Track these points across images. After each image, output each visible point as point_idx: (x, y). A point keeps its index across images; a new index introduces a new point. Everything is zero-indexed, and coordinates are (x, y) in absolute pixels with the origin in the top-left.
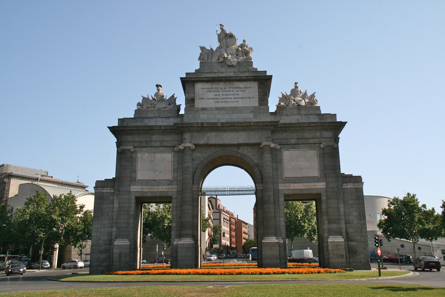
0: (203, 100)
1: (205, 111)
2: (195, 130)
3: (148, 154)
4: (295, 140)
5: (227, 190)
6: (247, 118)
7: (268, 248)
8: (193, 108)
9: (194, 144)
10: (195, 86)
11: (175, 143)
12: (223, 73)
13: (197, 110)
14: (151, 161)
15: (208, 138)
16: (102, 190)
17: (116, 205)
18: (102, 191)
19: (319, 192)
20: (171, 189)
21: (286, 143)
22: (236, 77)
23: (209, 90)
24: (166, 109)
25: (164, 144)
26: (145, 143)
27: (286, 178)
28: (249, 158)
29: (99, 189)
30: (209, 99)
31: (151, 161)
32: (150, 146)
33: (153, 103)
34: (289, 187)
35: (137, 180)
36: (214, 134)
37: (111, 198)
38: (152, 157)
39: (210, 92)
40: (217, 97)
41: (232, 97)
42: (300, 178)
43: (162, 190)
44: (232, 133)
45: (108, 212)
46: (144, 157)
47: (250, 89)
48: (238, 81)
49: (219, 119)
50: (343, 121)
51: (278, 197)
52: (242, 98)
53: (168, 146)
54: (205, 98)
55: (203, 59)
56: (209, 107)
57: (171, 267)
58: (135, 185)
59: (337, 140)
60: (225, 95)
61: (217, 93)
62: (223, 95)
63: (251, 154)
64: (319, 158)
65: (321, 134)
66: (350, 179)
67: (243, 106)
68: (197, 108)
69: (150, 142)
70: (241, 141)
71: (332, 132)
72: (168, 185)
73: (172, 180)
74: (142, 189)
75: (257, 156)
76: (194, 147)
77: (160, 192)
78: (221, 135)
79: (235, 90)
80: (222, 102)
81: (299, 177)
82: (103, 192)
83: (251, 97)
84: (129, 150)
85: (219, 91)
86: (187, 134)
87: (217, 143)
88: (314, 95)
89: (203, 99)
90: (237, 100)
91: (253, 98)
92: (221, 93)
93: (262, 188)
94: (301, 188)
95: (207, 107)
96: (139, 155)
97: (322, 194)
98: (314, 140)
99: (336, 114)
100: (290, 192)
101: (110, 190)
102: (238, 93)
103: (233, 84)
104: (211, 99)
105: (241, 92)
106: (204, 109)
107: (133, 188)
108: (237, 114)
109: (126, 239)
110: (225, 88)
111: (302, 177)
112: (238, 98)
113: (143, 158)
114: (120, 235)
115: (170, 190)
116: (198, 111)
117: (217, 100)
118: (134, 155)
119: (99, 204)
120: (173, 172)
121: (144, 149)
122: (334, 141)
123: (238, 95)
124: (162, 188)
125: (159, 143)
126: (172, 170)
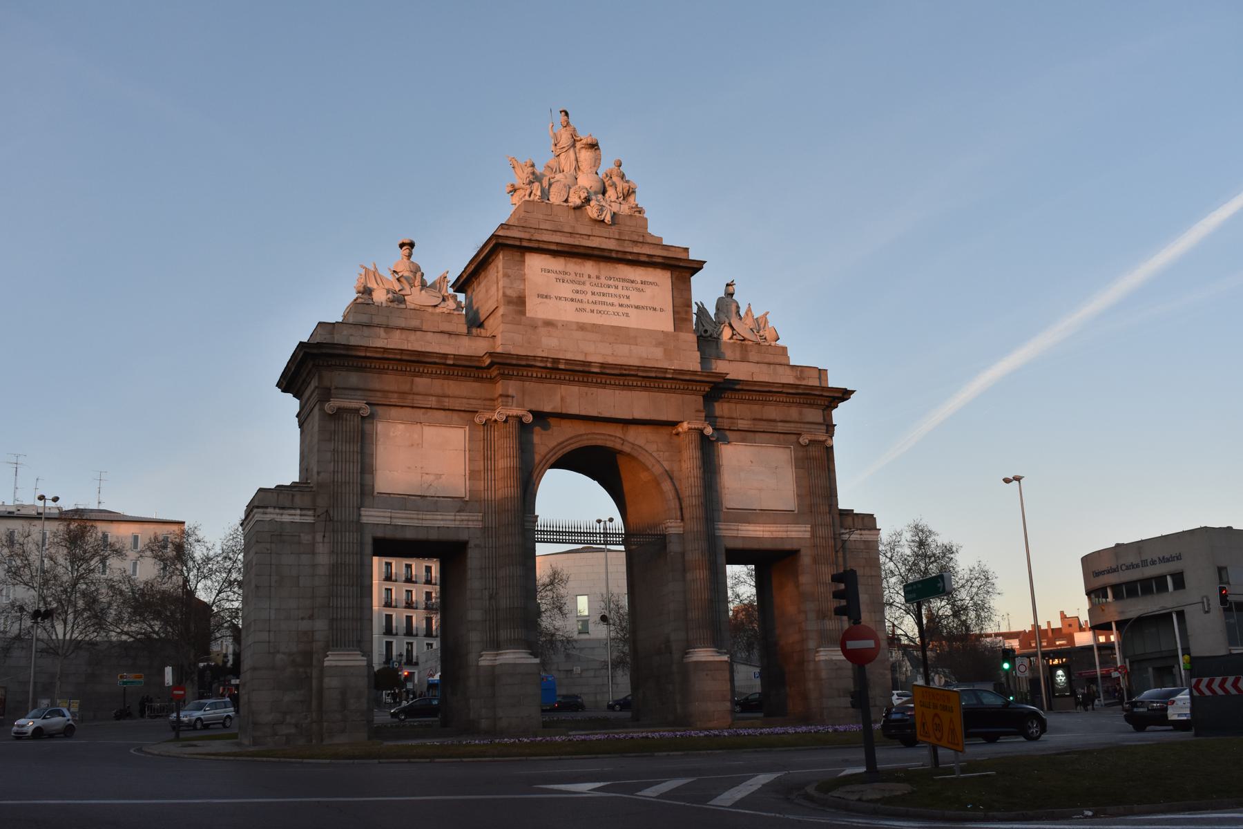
0: (547, 301)
1: (550, 329)
2: (532, 375)
3: (403, 426)
4: (745, 422)
5: (598, 531)
6: (649, 357)
7: (707, 675)
8: (523, 318)
9: (528, 411)
10: (524, 261)
11: (474, 404)
12: (591, 238)
13: (534, 325)
14: (412, 445)
15: (562, 399)
16: (277, 514)
17: (323, 558)
18: (278, 518)
19: (795, 547)
20: (465, 523)
21: (727, 428)
22: (617, 252)
23: (560, 276)
24: (438, 310)
25: (446, 404)
26: (396, 395)
27: (728, 509)
28: (651, 454)
29: (271, 513)
30: (560, 298)
31: (412, 445)
32: (411, 405)
33: (400, 291)
34: (736, 532)
35: (375, 494)
36: (575, 389)
37: (306, 538)
38: (416, 436)
39: (563, 282)
40: (579, 296)
41: (615, 301)
42: (758, 511)
43: (441, 524)
44: (617, 392)
45: (298, 577)
46: (394, 433)
47: (653, 286)
48: (627, 264)
49: (586, 354)
50: (848, 389)
51: (716, 556)
52: (637, 307)
53: (456, 408)
54: (552, 296)
55: (531, 192)
56: (564, 321)
57: (741, 712)
58: (373, 508)
59: (830, 428)
60: (599, 294)
61: (579, 288)
62: (593, 294)
63: (654, 447)
64: (795, 468)
65: (800, 414)
66: (853, 519)
67: (639, 327)
68: (532, 319)
69: (410, 394)
70: (639, 414)
71: (821, 411)
72: (457, 512)
73: (467, 499)
74: (391, 517)
75: (667, 454)
76: (529, 418)
77: (438, 527)
78: (592, 394)
79: (620, 284)
80: (592, 311)
81: (755, 510)
82: (282, 523)
83: (658, 308)
84: (357, 410)
85: (584, 283)
86: (512, 381)
87: (583, 413)
88: (766, 318)
89: (546, 297)
90: (625, 310)
91: (662, 310)
92: (587, 288)
93: (680, 531)
94: (760, 534)
95: (557, 318)
96: (380, 427)
97: (803, 552)
98: (787, 425)
99: (827, 370)
100: (739, 545)
101: (301, 515)
102: (625, 292)
103: (616, 268)
104: (566, 299)
105: (635, 292)
106: (549, 324)
107: (367, 513)
108: (628, 346)
109: (355, 650)
110: (598, 277)
111: (761, 510)
112: (628, 306)
113: (392, 434)
114: (337, 640)
115: (464, 524)
116: (536, 327)
117: (579, 305)
118: (367, 427)
119: (270, 553)
120: (469, 480)
121: (394, 412)
122: (825, 431)
123: (628, 297)
124: (444, 517)
125: (434, 398)
126: (467, 472)
